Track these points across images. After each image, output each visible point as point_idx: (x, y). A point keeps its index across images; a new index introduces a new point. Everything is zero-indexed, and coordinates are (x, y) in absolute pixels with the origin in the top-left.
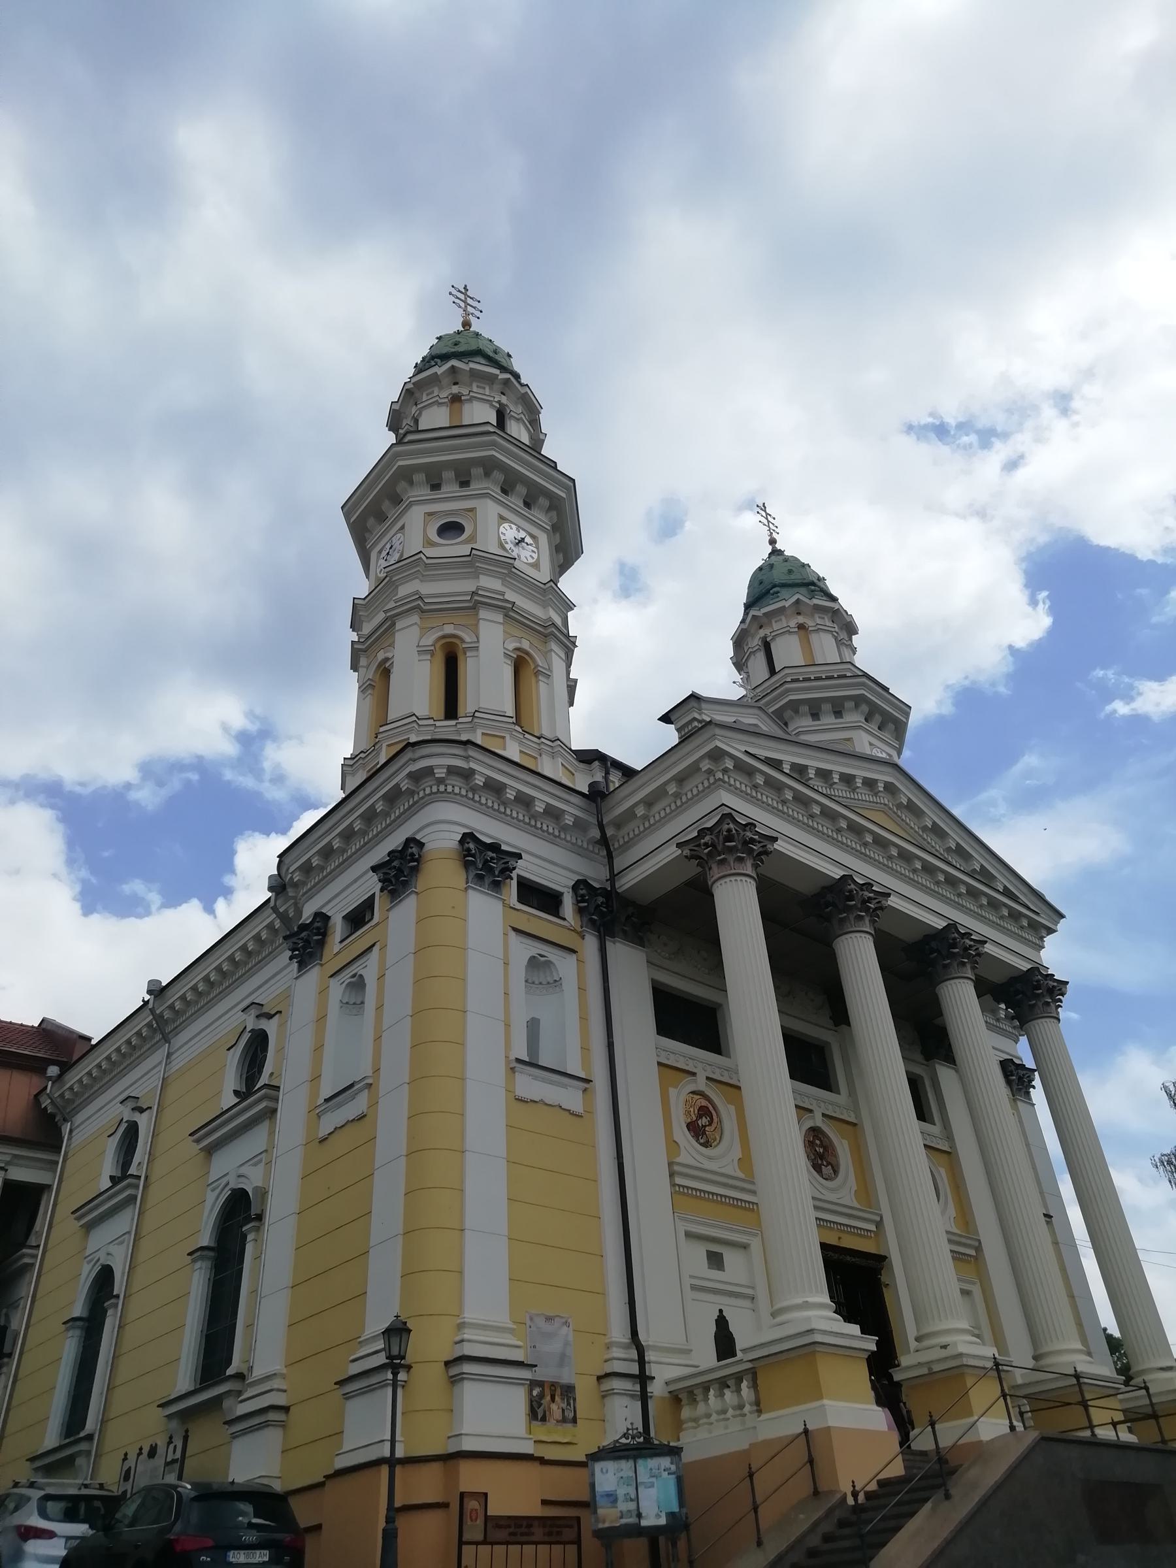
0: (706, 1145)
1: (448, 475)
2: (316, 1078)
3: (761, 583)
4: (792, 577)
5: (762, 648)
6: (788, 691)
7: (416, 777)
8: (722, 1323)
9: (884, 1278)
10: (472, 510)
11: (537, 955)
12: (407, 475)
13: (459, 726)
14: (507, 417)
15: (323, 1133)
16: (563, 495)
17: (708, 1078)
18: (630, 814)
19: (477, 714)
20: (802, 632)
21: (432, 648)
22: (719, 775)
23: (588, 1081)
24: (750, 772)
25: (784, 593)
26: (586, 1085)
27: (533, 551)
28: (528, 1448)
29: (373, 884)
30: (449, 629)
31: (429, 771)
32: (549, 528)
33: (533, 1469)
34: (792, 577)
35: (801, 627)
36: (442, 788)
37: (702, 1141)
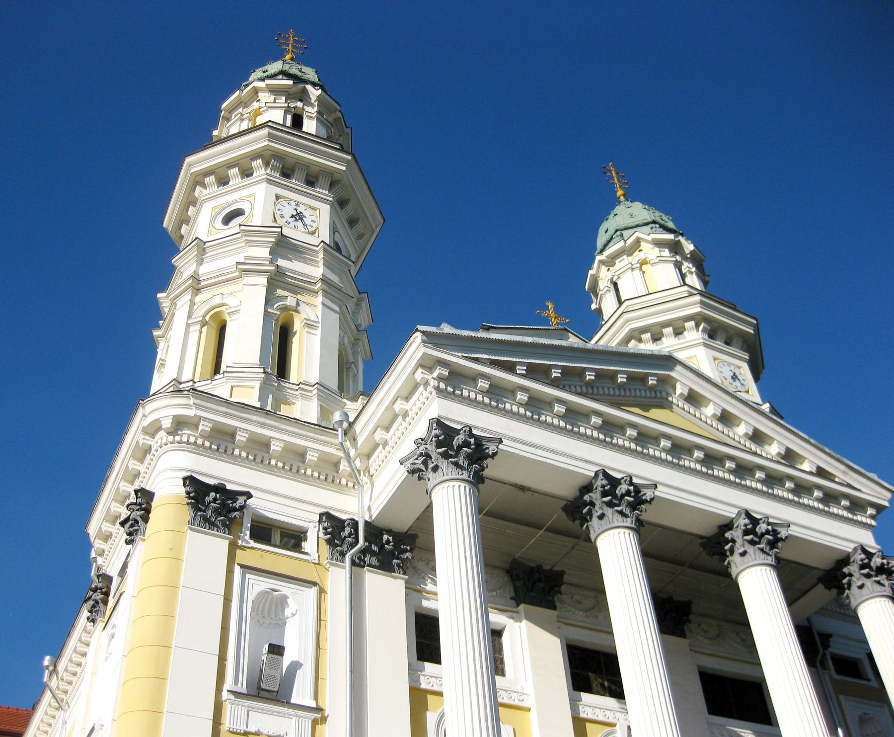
3: (606, 232)
4: (633, 220)
6: (628, 321)
11: (268, 590)
13: (214, 383)
19: (229, 369)
20: (644, 267)
21: (201, 319)
24: (472, 378)
25: (626, 233)
26: (313, 715)
27: (312, 221)
30: (217, 301)
32: (332, 199)
34: (633, 220)
35: (644, 262)
36: (171, 438)
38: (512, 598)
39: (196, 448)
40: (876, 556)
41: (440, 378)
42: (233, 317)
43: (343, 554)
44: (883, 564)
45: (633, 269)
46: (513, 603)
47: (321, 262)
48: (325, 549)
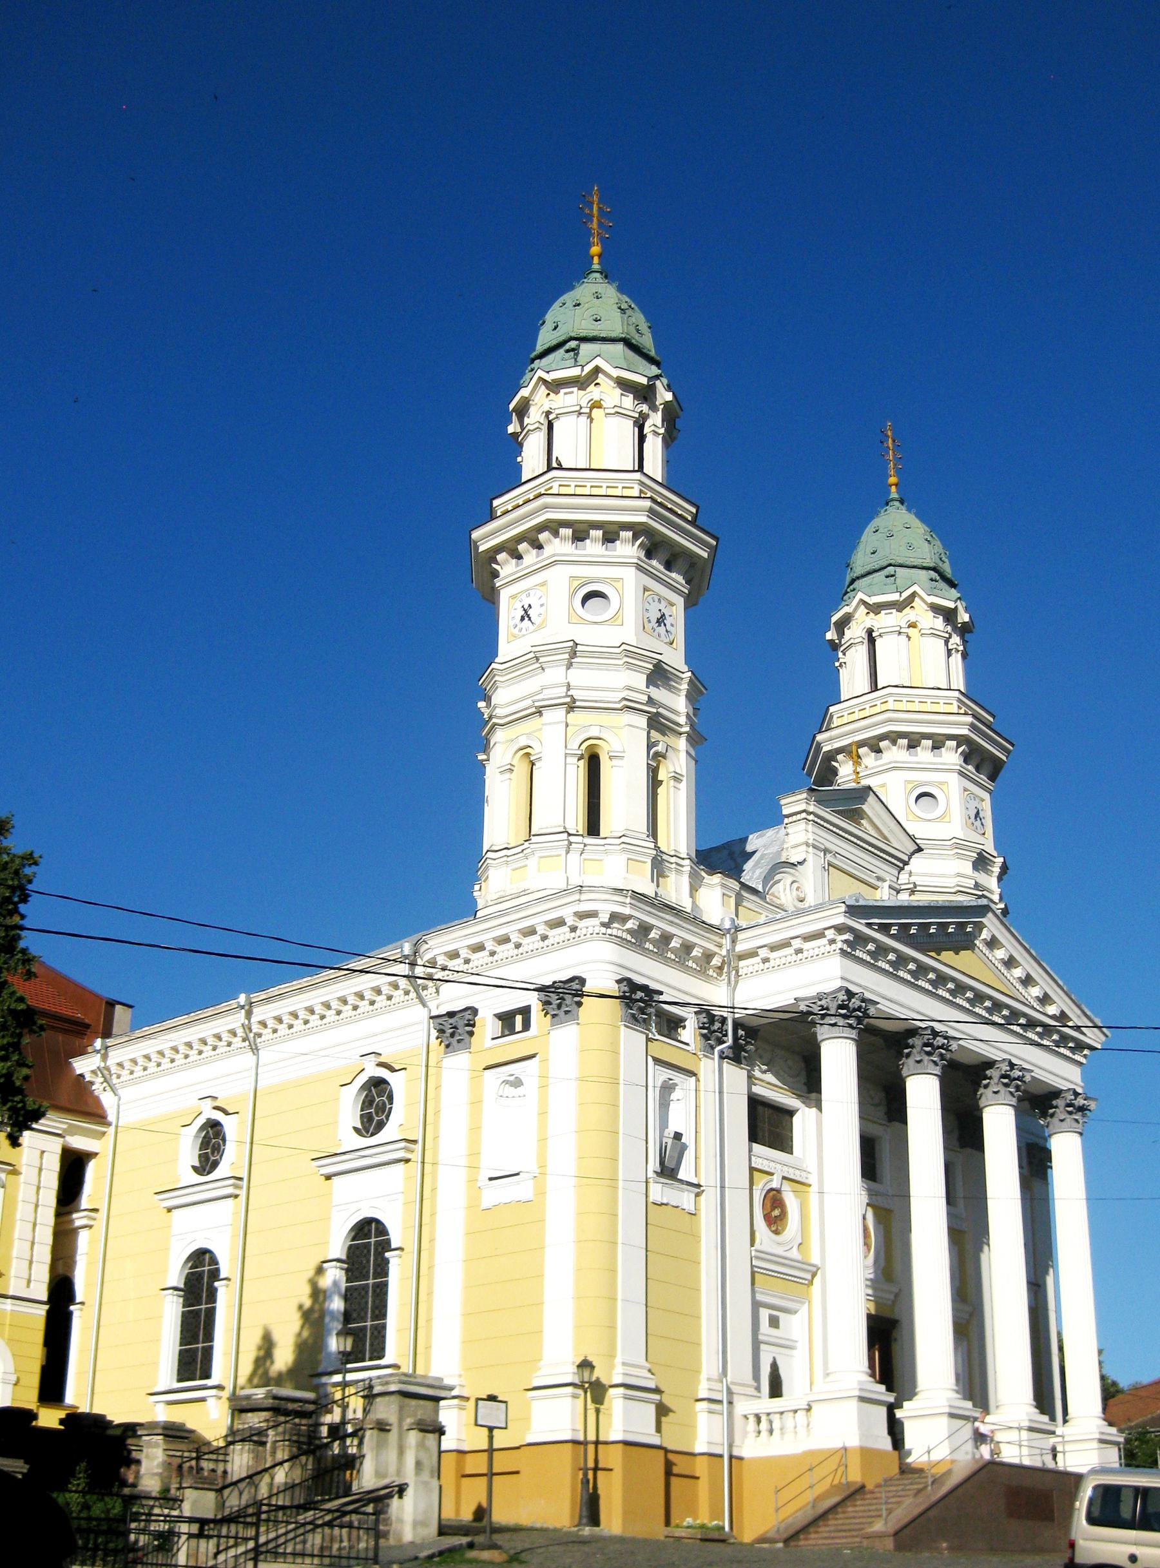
0: (776, 1232)
1: (597, 534)
2: (474, 1154)
4: (910, 553)
5: (866, 641)
7: (582, 916)
8: (775, 1367)
9: (895, 1334)
10: (617, 580)
12: (553, 527)
13: (607, 847)
14: (646, 430)
15: (484, 1205)
16: (705, 555)
17: (784, 1178)
18: (753, 954)
22: (839, 945)
23: (698, 1186)
28: (655, 1440)
29: (533, 1000)
30: (594, 732)
31: (593, 914)
32: (687, 591)
33: (662, 1453)
35: (912, 625)
36: (603, 930)
37: (773, 1229)
38: (805, 1084)
39: (621, 942)
40: (1081, 1096)
41: (846, 941)
42: (615, 762)
43: (712, 1048)
44: (1084, 1105)
45: (900, 633)
46: (805, 1088)
47: (684, 693)
48: (700, 1042)
